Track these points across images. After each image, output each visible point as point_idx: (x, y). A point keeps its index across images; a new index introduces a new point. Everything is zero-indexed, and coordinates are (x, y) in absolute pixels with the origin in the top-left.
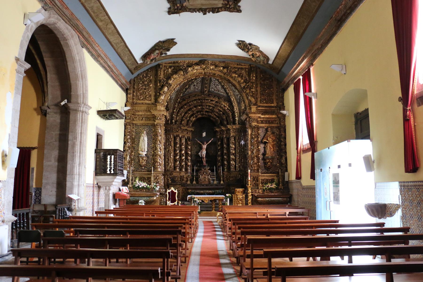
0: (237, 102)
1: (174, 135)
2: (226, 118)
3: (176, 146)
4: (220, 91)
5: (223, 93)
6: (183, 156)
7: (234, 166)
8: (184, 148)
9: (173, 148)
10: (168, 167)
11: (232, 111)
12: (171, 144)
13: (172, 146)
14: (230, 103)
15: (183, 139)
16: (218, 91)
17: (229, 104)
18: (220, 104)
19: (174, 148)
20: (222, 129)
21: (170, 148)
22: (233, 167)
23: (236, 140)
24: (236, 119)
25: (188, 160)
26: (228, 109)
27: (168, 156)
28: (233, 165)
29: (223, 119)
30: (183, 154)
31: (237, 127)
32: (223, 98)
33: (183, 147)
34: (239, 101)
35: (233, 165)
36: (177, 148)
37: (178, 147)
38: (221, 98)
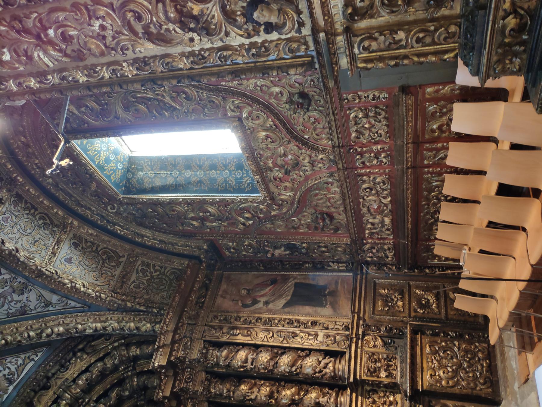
0: (76, 311)
2: (141, 374)
4: (13, 374)
5: (24, 364)
7: (327, 360)
11: (115, 341)
14: (81, 347)
16: (10, 382)
17: (82, 350)
18: (69, 387)
20: (168, 394)
22: (327, 364)
23: (225, 339)
24: (143, 329)
26: (101, 359)
28: (322, 364)
29: (145, 388)
31: (172, 327)
32: (48, 371)
34: (73, 304)
35: (322, 364)
38: (48, 378)
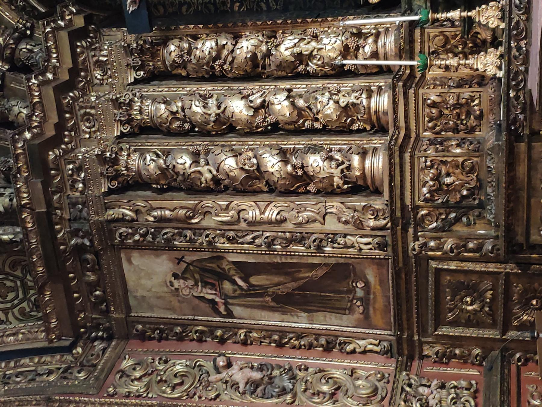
1: (110, 192)
3: (186, 177)
6: (265, 105)
8: (204, 98)
9: (208, 202)
10: (352, 246)
12: (176, 219)
13: (195, 211)
15: (141, 112)
19: (207, 191)
21: (208, 222)
25: (300, 58)
27: (270, 244)
30: (257, 110)
33: (197, 108)
36: (204, 169)
37: (196, 156)
